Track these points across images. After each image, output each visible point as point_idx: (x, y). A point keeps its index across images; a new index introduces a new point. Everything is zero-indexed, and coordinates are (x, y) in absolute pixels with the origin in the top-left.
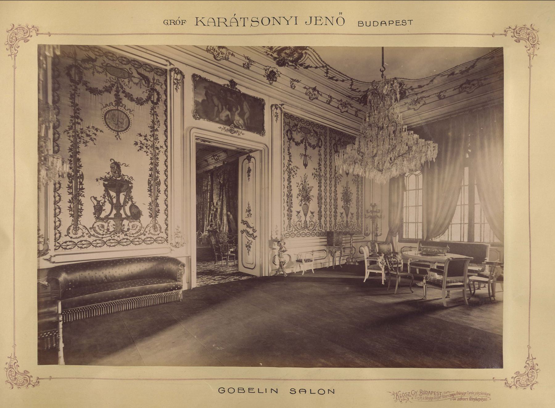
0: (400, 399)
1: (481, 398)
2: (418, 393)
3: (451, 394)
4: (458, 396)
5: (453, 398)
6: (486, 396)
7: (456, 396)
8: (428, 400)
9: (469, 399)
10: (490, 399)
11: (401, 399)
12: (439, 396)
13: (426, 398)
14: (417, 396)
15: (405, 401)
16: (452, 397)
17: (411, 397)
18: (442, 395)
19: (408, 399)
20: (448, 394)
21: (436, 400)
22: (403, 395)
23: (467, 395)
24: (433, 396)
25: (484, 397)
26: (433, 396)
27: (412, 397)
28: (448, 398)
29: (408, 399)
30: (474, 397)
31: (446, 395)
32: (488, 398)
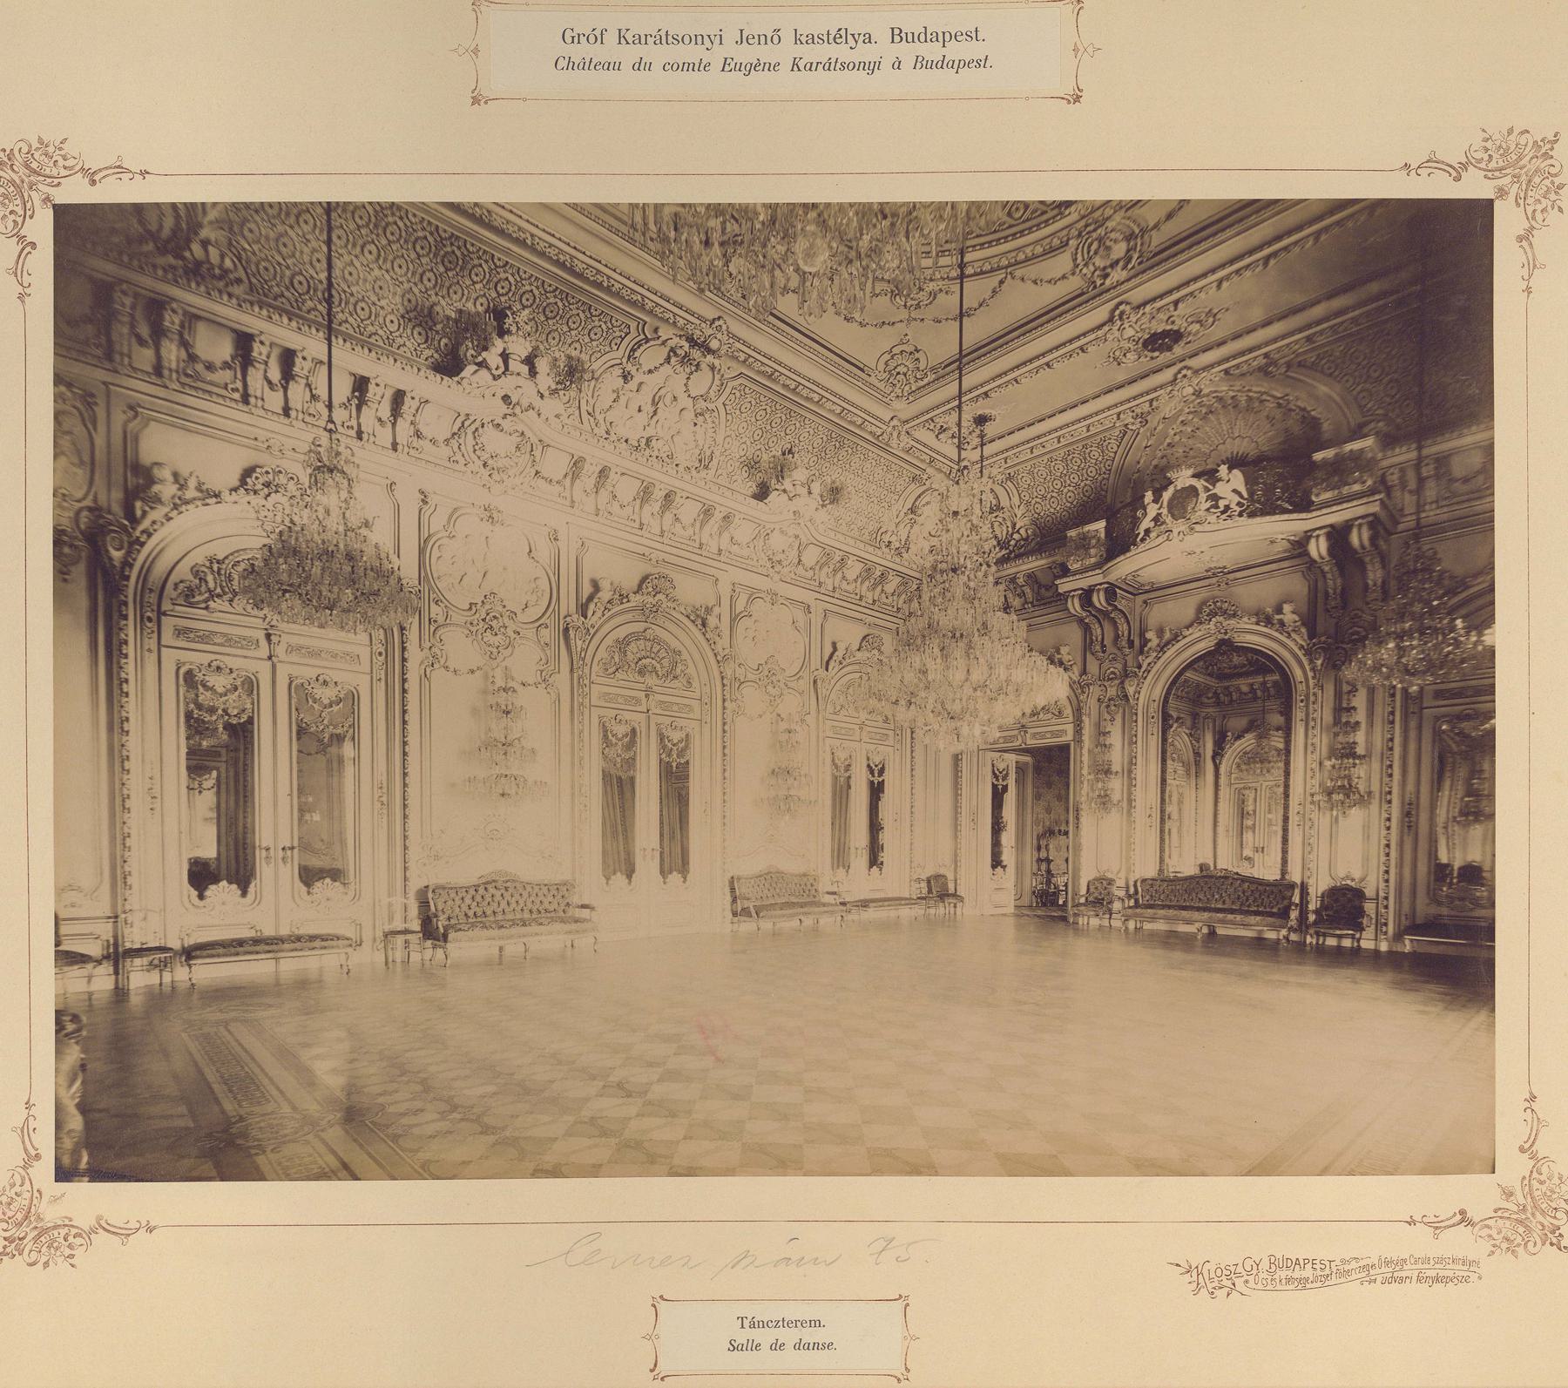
0: (1210, 1286)
1: (1447, 1273)
2: (1265, 1265)
3: (1362, 1263)
4: (1383, 1270)
5: (1368, 1279)
6: (1465, 1268)
7: (1378, 1271)
8: (1292, 1287)
9: (1415, 1278)
10: (1480, 1278)
11: (1214, 1285)
12: (1327, 1271)
13: (1289, 1280)
14: (1261, 1275)
15: (1226, 1290)
16: (1364, 1274)
17: (1243, 1279)
18: (1334, 1270)
19: (1234, 1284)
20: (1354, 1265)
21: (1319, 1284)
22: (1219, 1271)
23: (1409, 1267)
24: (1308, 1272)
25: (1460, 1269)
26: (1308, 1272)
27: (1246, 1277)
28: (1354, 1276)
29: (1234, 1284)
30: (1432, 1273)
31: (1350, 1267)
32: (1468, 1274)
